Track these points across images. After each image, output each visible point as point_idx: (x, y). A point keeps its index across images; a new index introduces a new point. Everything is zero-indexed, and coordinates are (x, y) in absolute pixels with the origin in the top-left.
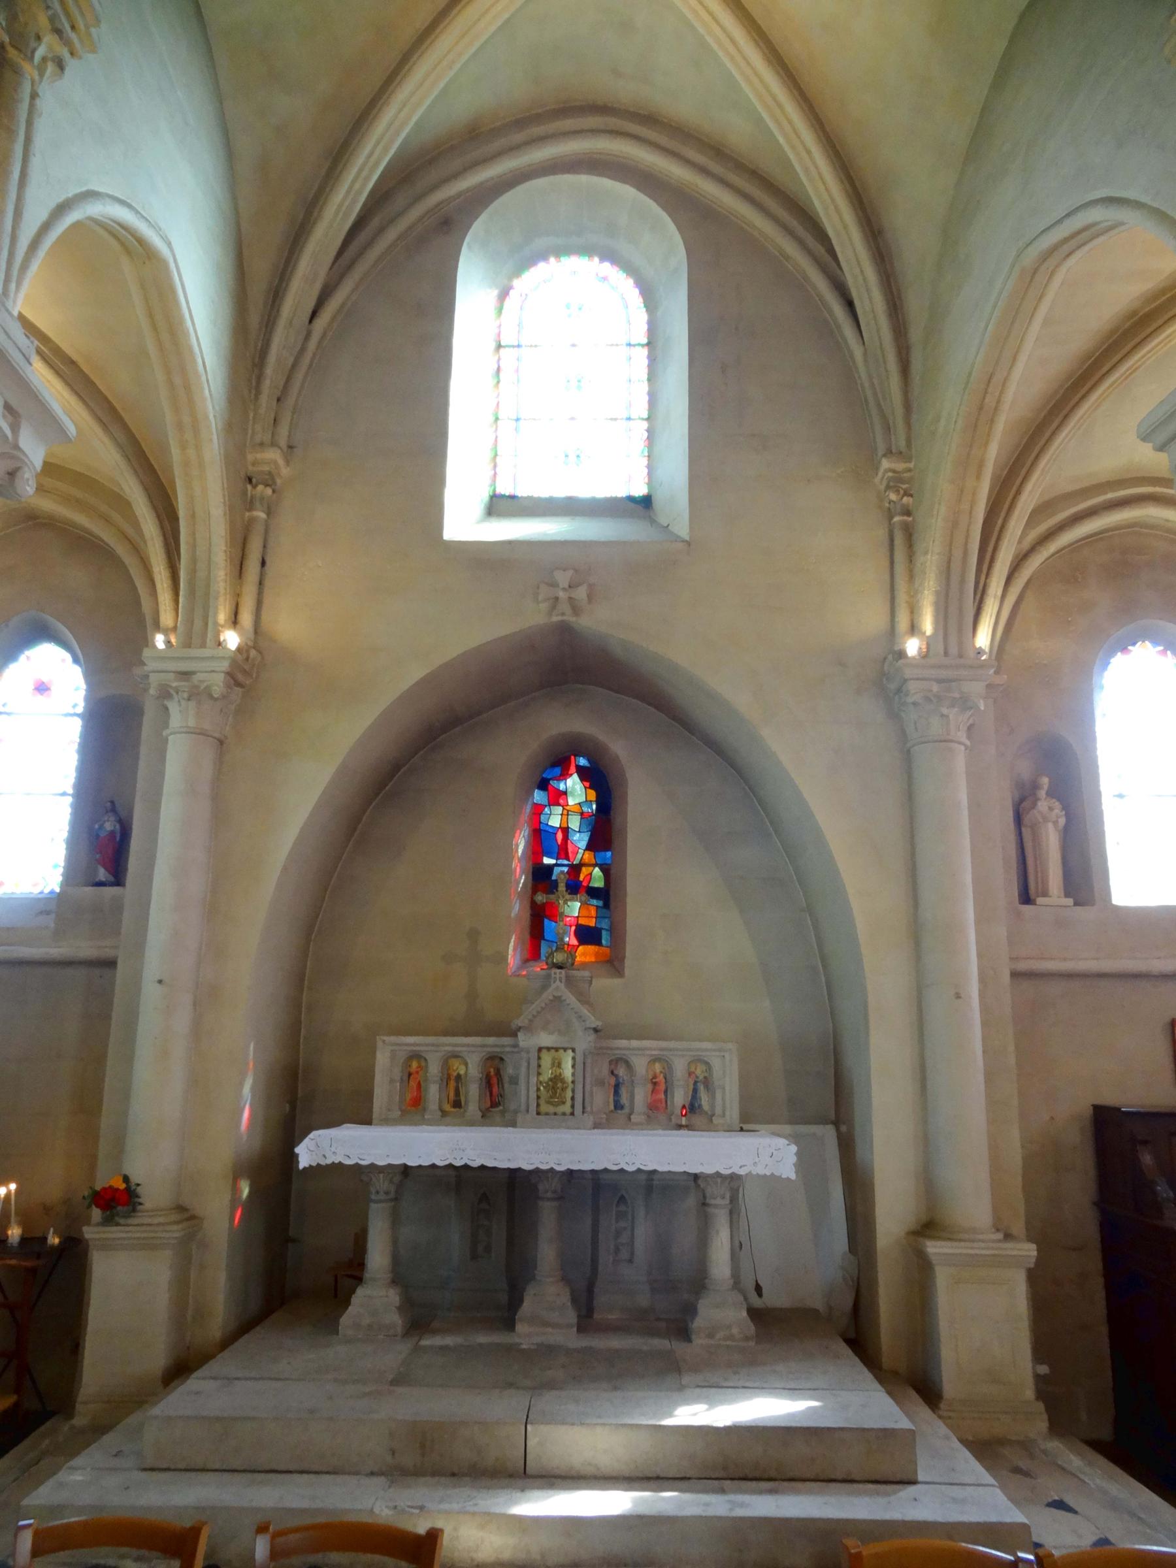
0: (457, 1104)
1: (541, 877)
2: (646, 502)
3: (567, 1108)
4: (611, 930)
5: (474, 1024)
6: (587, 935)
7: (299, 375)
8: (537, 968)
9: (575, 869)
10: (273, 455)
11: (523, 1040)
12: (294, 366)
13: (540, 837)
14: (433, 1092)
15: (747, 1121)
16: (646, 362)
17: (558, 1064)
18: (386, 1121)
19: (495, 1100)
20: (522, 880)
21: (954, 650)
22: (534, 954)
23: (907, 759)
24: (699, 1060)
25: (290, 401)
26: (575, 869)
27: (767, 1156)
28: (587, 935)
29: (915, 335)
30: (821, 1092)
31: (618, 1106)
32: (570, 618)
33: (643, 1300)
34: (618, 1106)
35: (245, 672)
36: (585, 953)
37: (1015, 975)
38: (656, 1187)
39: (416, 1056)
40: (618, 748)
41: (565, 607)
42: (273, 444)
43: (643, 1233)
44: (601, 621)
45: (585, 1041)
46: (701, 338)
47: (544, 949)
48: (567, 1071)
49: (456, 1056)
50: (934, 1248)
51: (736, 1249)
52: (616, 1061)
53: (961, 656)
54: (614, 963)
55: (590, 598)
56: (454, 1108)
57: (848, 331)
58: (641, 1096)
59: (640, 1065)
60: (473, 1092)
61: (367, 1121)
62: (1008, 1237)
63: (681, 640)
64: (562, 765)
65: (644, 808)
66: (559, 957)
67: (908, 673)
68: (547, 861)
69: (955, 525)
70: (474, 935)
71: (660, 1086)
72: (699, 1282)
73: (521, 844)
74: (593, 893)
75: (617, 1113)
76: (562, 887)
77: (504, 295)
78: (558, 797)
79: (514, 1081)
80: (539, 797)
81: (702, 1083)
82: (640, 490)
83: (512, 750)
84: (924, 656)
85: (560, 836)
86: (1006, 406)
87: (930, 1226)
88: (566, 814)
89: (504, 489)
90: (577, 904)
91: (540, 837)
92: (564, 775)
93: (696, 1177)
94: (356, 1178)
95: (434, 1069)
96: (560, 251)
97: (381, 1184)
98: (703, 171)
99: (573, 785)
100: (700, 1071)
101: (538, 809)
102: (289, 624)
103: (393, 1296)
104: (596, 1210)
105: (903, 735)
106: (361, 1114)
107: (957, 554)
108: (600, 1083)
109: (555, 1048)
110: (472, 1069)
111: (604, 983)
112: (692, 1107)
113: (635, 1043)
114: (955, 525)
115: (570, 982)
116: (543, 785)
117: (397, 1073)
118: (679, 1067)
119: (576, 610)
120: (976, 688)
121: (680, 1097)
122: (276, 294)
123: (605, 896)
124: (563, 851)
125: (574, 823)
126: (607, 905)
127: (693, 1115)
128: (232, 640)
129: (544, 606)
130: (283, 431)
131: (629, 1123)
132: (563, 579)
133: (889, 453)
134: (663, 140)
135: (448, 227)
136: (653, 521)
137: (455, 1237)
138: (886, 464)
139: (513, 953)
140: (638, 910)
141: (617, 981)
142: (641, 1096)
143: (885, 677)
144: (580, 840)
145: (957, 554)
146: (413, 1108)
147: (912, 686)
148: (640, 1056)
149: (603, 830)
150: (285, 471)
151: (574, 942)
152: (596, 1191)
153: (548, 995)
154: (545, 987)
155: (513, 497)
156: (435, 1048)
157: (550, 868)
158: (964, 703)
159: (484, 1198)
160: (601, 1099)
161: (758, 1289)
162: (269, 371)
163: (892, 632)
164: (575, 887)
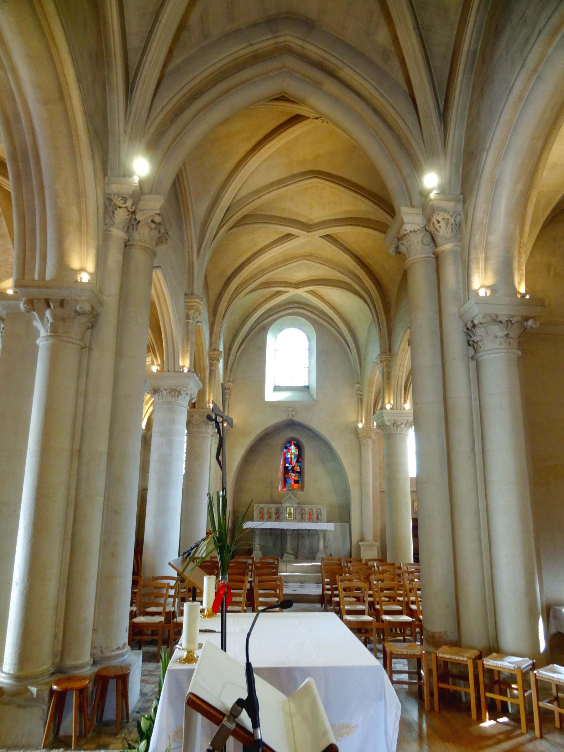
0: (270, 518)
1: (286, 468)
2: (308, 387)
3: (292, 518)
4: (301, 480)
5: (272, 501)
6: (296, 482)
7: (235, 365)
9: (293, 467)
10: (230, 384)
11: (283, 505)
12: (233, 363)
13: (286, 460)
14: (266, 516)
15: (329, 521)
16: (308, 354)
17: (290, 510)
18: (256, 521)
19: (278, 517)
20: (281, 469)
21: (368, 427)
22: (284, 486)
23: (360, 447)
24: (318, 509)
25: (233, 371)
26: (293, 467)
27: (330, 527)
28: (296, 482)
29: (362, 357)
30: (343, 515)
31: (302, 518)
32: (292, 418)
33: (308, 555)
34: (302, 518)
36: (296, 486)
37: (380, 492)
38: (310, 533)
39: (262, 508)
40: (302, 440)
41: (290, 415)
42: (230, 382)
43: (307, 542)
44: (297, 418)
45: (296, 505)
46: (319, 355)
47: (287, 485)
48: (292, 511)
49: (270, 508)
50: (360, 543)
51: (326, 547)
52: (302, 509)
53: (370, 428)
54: (302, 488)
55: (296, 414)
56: (270, 519)
57: (350, 354)
59: (307, 510)
60: (274, 516)
61: (253, 521)
62: (376, 542)
63: (314, 421)
64: (290, 442)
65: (308, 454)
66: (290, 488)
67: (359, 431)
68: (287, 465)
69: (368, 402)
70: (271, 482)
71: (311, 515)
72: (318, 550)
74: (297, 472)
75: (302, 519)
76: (291, 471)
77: (276, 338)
78: (289, 450)
79: (282, 513)
80: (285, 450)
81: (319, 514)
82: (307, 384)
83: (280, 440)
84: (363, 428)
85: (290, 460)
86: (375, 381)
87: (362, 540)
88: (291, 454)
89: (277, 385)
90: (294, 474)
91: (286, 460)
92: (291, 445)
93: (316, 530)
94: (253, 531)
95: (266, 511)
96: (288, 328)
97: (258, 532)
98: (319, 317)
99: (293, 447)
100: (319, 511)
101: (285, 453)
103: (260, 552)
104: (298, 539)
105: (360, 442)
107: (369, 407)
108: (299, 513)
110: (273, 511)
111: (300, 493)
112: (317, 519)
113: (306, 506)
114: (368, 402)
115: (292, 493)
116: (286, 448)
117: (258, 511)
118: (315, 511)
119: (293, 416)
120: (373, 434)
121: (315, 516)
122: (230, 349)
123: (300, 473)
124: (290, 463)
125: (293, 457)
126: (300, 475)
127: (318, 520)
129: (287, 415)
130: (232, 378)
131: (304, 521)
132: (290, 409)
133: (358, 383)
134: (310, 310)
135: (265, 329)
136: (309, 393)
137: (271, 544)
138: (357, 385)
140: (307, 477)
141: (303, 492)
142: (307, 516)
143: (356, 431)
144: (294, 461)
145: (369, 407)
146: (261, 518)
147: (360, 434)
148: (307, 508)
149: (300, 457)
150: (232, 386)
151: (293, 483)
152: (298, 533)
153: (288, 496)
154: (287, 494)
155: (279, 386)
156: (266, 507)
157: (288, 467)
158: (370, 437)
159: (276, 536)
160: (299, 517)
161: (331, 555)
162: (229, 366)
163: (357, 422)
164: (293, 471)
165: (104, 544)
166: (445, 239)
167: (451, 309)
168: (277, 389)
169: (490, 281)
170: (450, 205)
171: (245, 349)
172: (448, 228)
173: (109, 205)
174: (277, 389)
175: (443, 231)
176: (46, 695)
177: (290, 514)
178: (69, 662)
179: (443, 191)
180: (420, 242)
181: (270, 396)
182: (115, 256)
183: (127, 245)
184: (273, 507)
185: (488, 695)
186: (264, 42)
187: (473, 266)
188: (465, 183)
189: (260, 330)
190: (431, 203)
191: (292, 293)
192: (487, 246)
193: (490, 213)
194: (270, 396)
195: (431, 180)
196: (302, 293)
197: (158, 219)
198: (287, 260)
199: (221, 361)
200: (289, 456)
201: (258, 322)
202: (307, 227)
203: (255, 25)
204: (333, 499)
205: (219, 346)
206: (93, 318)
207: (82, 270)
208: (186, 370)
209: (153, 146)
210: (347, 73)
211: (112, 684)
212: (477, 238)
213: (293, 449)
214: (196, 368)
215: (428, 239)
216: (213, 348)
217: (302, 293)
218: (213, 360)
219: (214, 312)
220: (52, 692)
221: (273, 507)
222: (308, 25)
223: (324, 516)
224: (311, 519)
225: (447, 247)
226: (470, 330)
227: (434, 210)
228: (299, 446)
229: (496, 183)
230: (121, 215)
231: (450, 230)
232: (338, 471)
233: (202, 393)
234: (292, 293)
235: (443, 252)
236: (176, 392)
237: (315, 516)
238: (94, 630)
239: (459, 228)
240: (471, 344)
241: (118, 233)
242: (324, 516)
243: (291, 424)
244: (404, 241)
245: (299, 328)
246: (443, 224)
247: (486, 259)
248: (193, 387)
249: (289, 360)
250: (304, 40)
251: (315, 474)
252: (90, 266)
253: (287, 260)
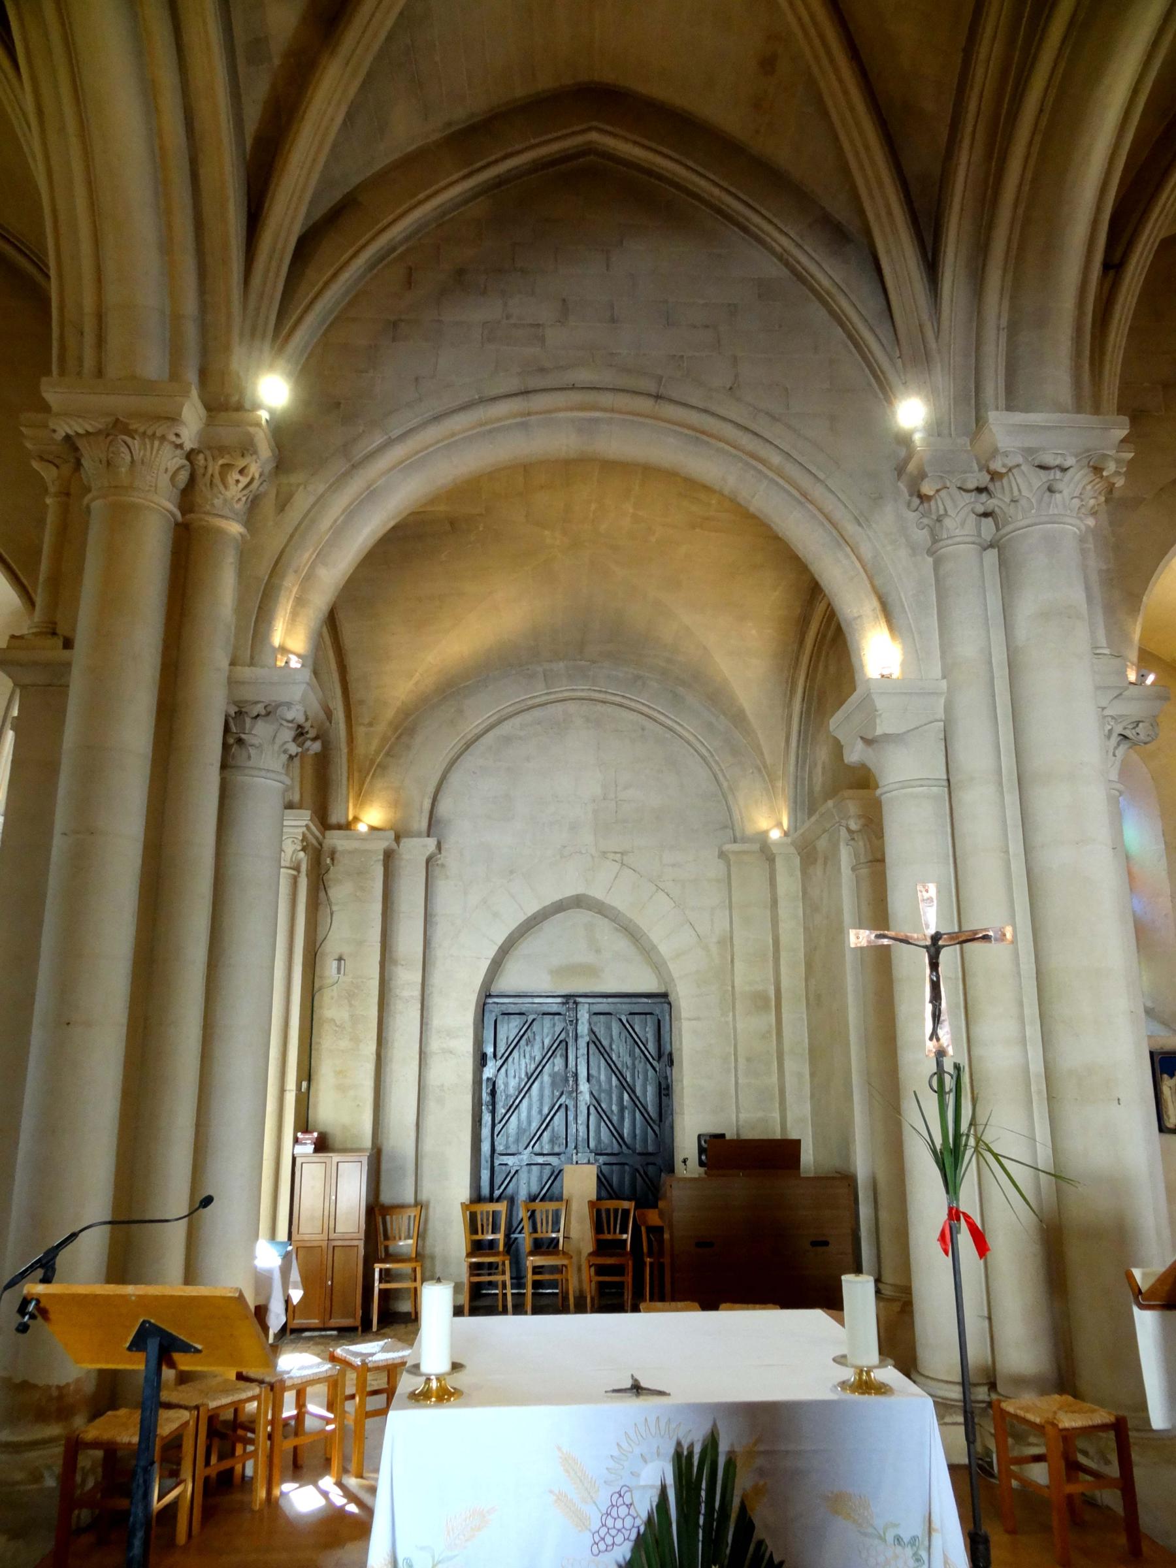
166: (232, 509)
172: (245, 492)
180: (170, 474)
190: (252, 430)
192: (308, 579)
193: (339, 531)
195: (273, 391)
212: (304, 557)
215: (183, 477)
227: (247, 448)
229: (371, 495)
231: (244, 499)
235: (220, 532)
240: (233, 742)
244: (136, 444)
246: (244, 481)
247: (300, 602)
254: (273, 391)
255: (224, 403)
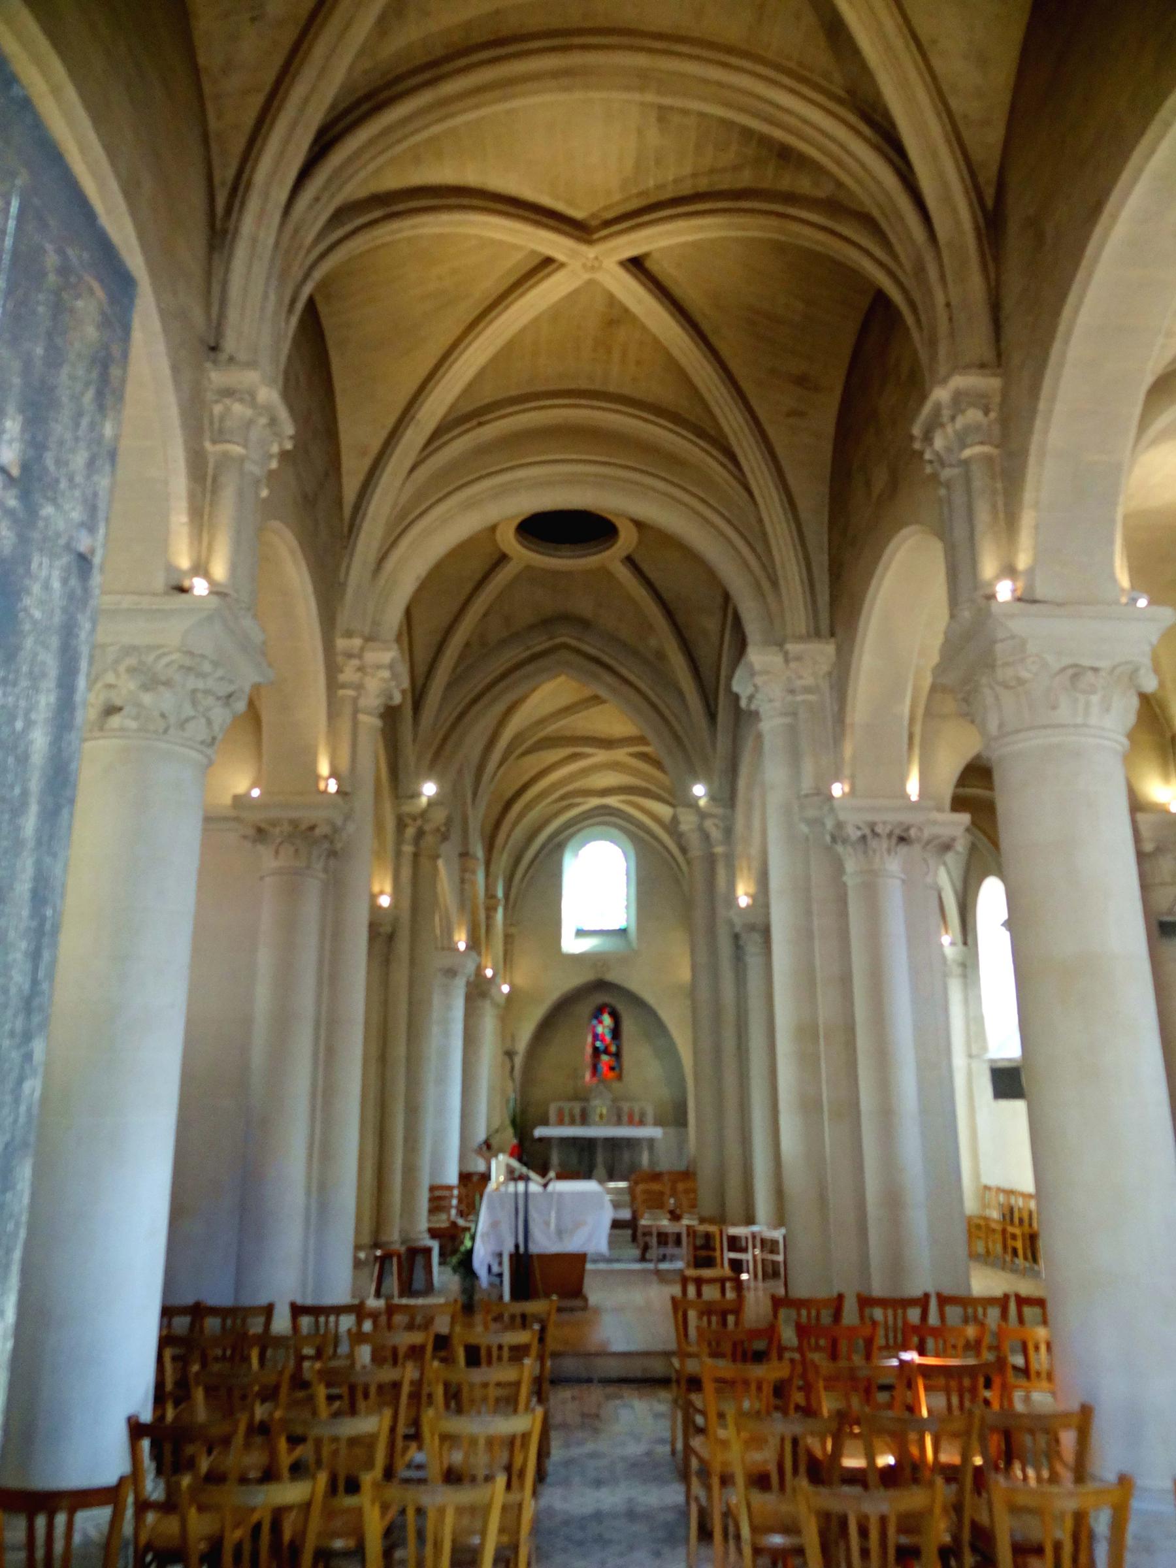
8: (595, 1080)
13: (596, 1037)
14: (567, 1119)
19: (584, 1120)
20: (589, 1050)
28: (612, 1069)
30: (676, 1117)
35: (509, 997)
36: (611, 1074)
40: (621, 1008)
43: (626, 1156)
44: (612, 977)
45: (609, 1103)
54: (620, 1077)
56: (573, 1122)
58: (625, 1118)
60: (578, 1118)
63: (636, 981)
73: (590, 1039)
75: (619, 1123)
78: (601, 1022)
80: (595, 1022)
81: (643, 1115)
83: (585, 1008)
90: (609, 1057)
91: (596, 1037)
101: (594, 1027)
102: (520, 979)
106: (545, 1122)
109: (600, 1106)
110: (577, 1111)
111: (616, 1085)
121: (637, 1118)
123: (617, 1055)
124: (603, 1040)
125: (607, 1031)
127: (641, 1123)
128: (505, 989)
139: (588, 1076)
142: (625, 1118)
144: (608, 1037)
146: (561, 1122)
148: (626, 1107)
149: (616, 1033)
156: (567, 1106)
164: (606, 1051)
165: (406, 1140)
167: (722, 912)
168: (580, 933)
169: (752, 890)
170: (719, 811)
171: (531, 885)
173: (401, 825)
174: (580, 933)
175: (716, 834)
176: (372, 1259)
177: (601, 1116)
178: (384, 1238)
179: (713, 798)
181: (571, 945)
182: (406, 872)
183: (416, 855)
184: (577, 1107)
185: (733, 1255)
186: (540, 643)
187: (738, 874)
188: (727, 796)
189: (554, 850)
191: (595, 802)
194: (571, 945)
196: (612, 801)
197: (443, 829)
198: (585, 772)
199: (500, 911)
200: (600, 1030)
201: (551, 838)
202: (607, 743)
203: (531, 627)
204: (663, 1093)
205: (496, 890)
206: (391, 937)
207: (382, 893)
208: (462, 946)
209: (436, 763)
210: (624, 672)
211: (420, 1261)
213: (607, 1019)
214: (474, 944)
216: (490, 895)
217: (612, 801)
218: (490, 910)
219: (490, 848)
220: (376, 1258)
221: (577, 1107)
222: (584, 624)
223: (650, 1117)
224: (631, 1122)
225: (719, 850)
226: (736, 937)
228: (615, 1016)
230: (410, 832)
232: (669, 1053)
233: (479, 970)
234: (595, 802)
236: (451, 973)
237: (637, 1118)
238: (401, 1216)
239: (728, 832)
241: (408, 849)
242: (650, 1117)
243: (601, 985)
245: (611, 841)
248: (470, 967)
249: (596, 890)
250: (579, 639)
251: (639, 1057)
252: (388, 888)
253: (585, 772)
254: (699, 790)
255: (692, 804)
